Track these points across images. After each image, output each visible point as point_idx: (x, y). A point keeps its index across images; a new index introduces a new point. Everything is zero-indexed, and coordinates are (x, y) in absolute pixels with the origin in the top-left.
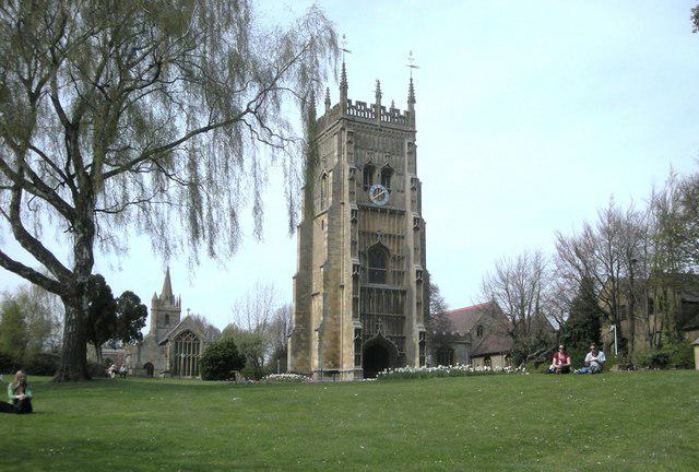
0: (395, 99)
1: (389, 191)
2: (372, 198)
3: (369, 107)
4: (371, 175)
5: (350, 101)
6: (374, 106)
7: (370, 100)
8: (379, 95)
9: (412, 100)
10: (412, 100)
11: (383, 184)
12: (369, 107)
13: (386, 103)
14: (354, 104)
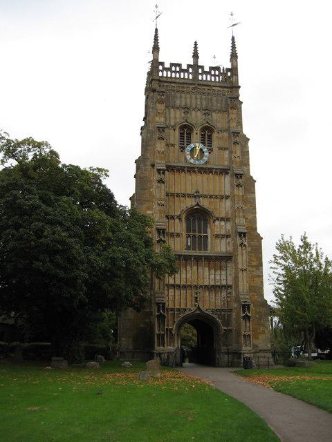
0: (214, 57)
1: (211, 151)
2: (189, 157)
3: (184, 67)
4: (189, 135)
5: (162, 64)
6: (189, 66)
7: (186, 60)
8: (196, 56)
9: (234, 56)
10: (234, 56)
11: (204, 143)
12: (184, 67)
13: (206, 62)
14: (167, 65)
